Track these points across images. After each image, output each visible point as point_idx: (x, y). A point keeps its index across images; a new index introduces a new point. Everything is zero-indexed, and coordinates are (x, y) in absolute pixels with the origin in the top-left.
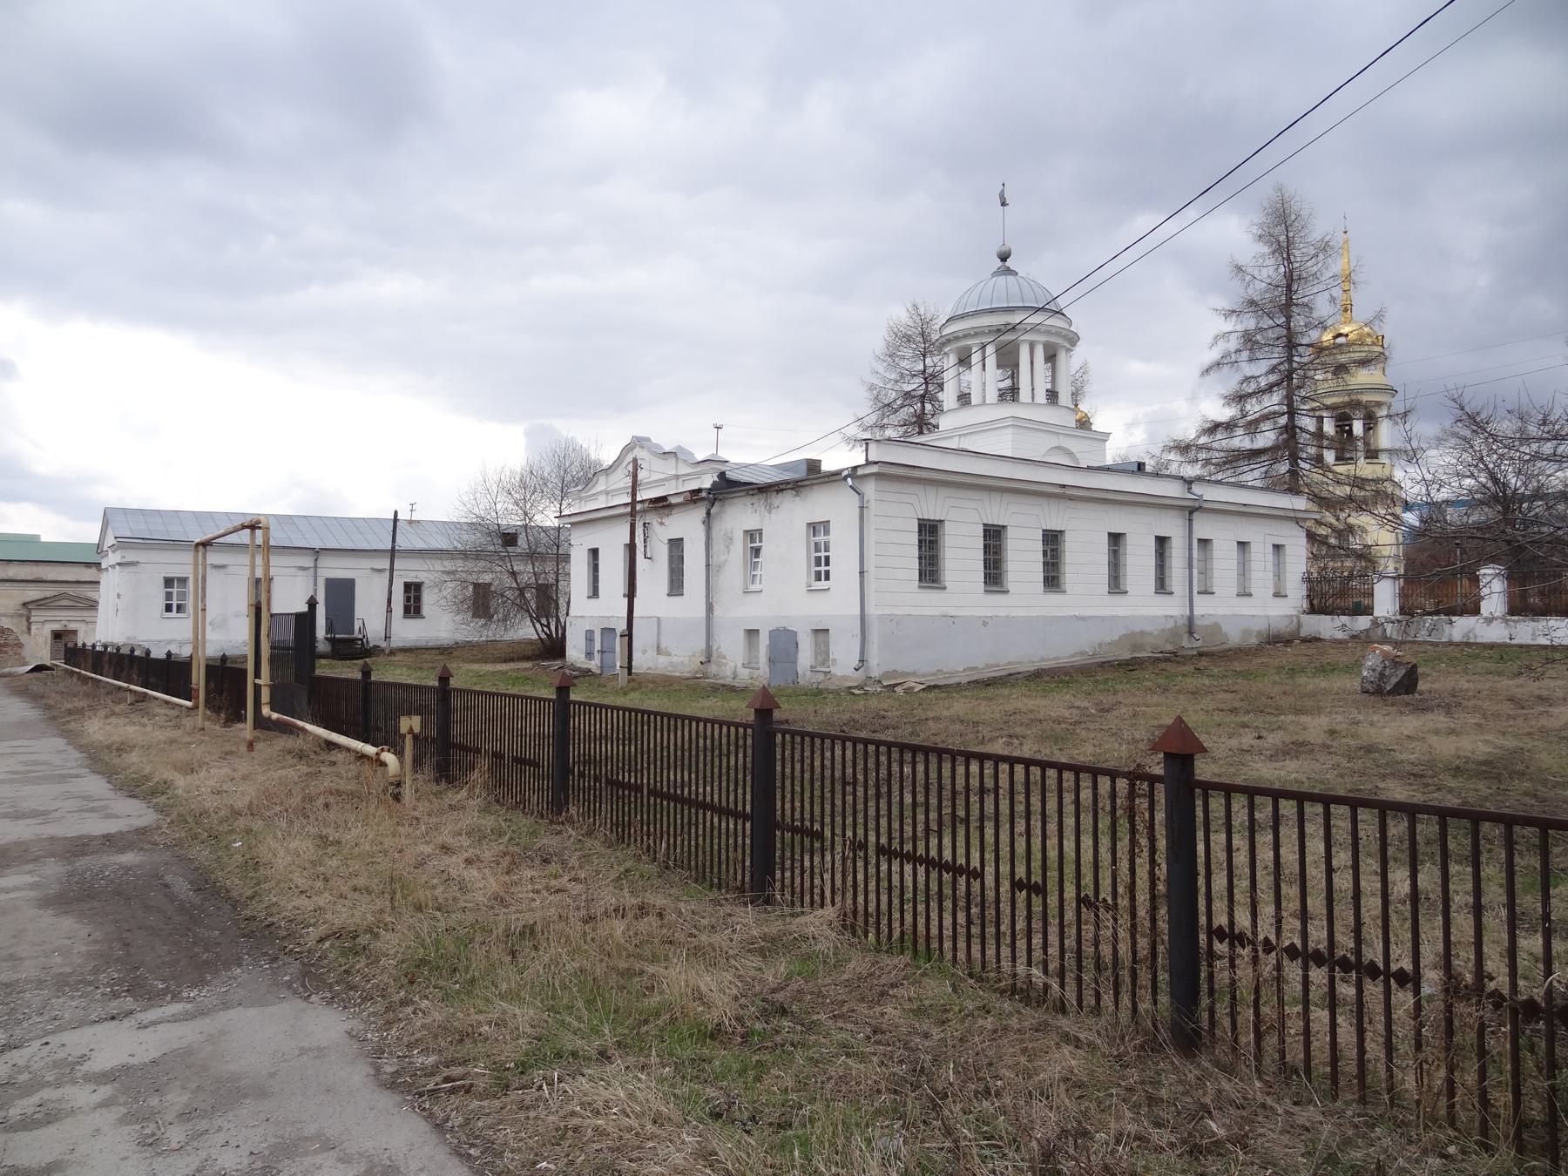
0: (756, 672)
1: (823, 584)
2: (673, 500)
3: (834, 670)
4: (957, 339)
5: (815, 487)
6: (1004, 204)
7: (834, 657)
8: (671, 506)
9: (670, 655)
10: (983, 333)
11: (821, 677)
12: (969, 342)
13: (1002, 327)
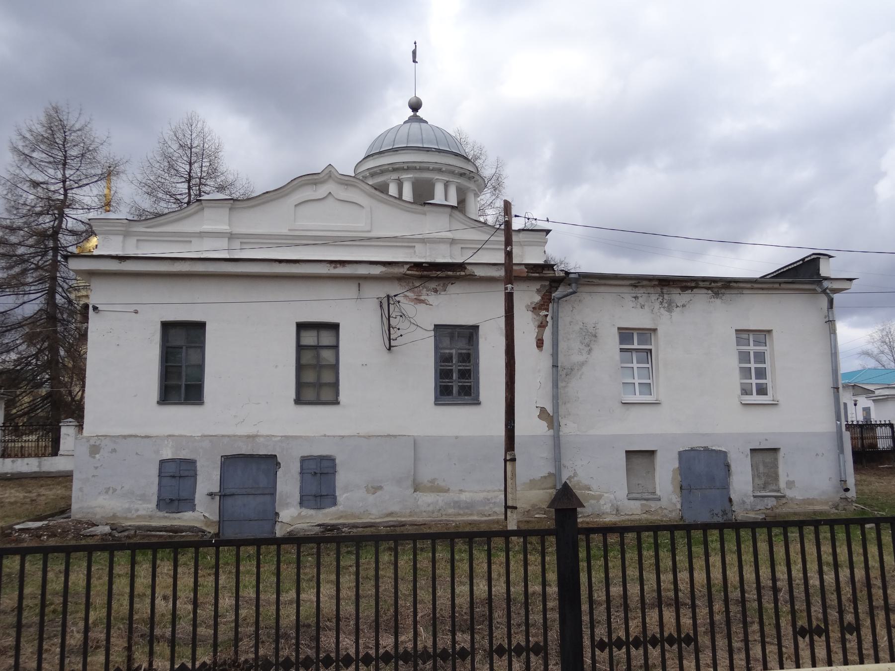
0: (653, 505)
1: (755, 398)
2: (479, 272)
3: (789, 493)
4: (421, 169)
5: (745, 291)
6: (414, 61)
7: (791, 478)
8: (472, 279)
9: (447, 491)
10: (452, 173)
11: (771, 503)
12: (436, 176)
13: (468, 173)
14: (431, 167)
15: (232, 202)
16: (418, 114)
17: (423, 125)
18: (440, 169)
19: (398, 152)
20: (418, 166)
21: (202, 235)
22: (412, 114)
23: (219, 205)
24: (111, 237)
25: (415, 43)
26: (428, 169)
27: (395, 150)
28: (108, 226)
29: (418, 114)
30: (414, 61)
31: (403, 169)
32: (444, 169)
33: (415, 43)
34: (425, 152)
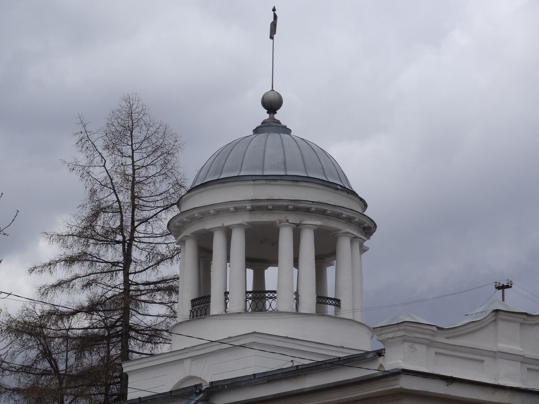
14: (314, 208)
15: (525, 317)
16: (276, 116)
17: (285, 136)
18: (338, 215)
19: (298, 184)
20: (329, 210)
21: (495, 355)
22: (267, 116)
23: (511, 318)
24: (416, 346)
25: (274, 10)
26: (338, 217)
27: (296, 180)
28: (419, 333)
29: (276, 116)
30: (272, 37)
31: (308, 211)
32: (313, 209)
33: (274, 10)
34: (334, 190)
